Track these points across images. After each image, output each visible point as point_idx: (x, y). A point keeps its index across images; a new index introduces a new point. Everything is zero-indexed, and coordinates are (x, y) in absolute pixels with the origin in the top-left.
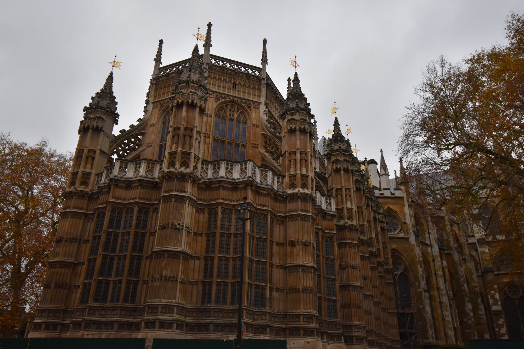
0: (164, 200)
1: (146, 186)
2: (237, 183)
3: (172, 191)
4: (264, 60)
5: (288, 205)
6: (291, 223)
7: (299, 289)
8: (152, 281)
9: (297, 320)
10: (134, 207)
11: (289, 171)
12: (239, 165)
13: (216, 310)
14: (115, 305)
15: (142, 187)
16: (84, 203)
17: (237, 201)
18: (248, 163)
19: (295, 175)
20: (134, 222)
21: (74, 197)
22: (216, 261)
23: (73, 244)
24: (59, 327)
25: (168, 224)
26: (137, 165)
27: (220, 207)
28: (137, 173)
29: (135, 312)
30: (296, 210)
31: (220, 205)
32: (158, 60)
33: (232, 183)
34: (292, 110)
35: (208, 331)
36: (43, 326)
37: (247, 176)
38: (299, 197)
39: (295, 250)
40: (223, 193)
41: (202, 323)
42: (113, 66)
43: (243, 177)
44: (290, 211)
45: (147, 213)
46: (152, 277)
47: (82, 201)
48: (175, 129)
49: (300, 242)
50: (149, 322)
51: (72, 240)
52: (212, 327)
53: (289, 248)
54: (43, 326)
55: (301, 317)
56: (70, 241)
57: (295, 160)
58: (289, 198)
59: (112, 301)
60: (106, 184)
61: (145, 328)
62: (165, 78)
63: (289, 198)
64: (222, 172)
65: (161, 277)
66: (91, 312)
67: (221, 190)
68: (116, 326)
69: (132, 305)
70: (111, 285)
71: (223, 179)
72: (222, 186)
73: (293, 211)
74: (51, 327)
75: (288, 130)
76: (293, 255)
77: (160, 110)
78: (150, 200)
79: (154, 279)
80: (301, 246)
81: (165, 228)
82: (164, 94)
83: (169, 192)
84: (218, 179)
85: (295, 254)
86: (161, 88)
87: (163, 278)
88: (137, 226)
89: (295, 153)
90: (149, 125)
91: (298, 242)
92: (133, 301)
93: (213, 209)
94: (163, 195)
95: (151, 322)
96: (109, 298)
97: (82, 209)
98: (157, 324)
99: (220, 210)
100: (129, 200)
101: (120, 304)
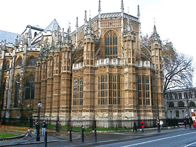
4: (138, 15)
20: (117, 80)
45: (119, 77)
88: (118, 81)
92: (120, 104)
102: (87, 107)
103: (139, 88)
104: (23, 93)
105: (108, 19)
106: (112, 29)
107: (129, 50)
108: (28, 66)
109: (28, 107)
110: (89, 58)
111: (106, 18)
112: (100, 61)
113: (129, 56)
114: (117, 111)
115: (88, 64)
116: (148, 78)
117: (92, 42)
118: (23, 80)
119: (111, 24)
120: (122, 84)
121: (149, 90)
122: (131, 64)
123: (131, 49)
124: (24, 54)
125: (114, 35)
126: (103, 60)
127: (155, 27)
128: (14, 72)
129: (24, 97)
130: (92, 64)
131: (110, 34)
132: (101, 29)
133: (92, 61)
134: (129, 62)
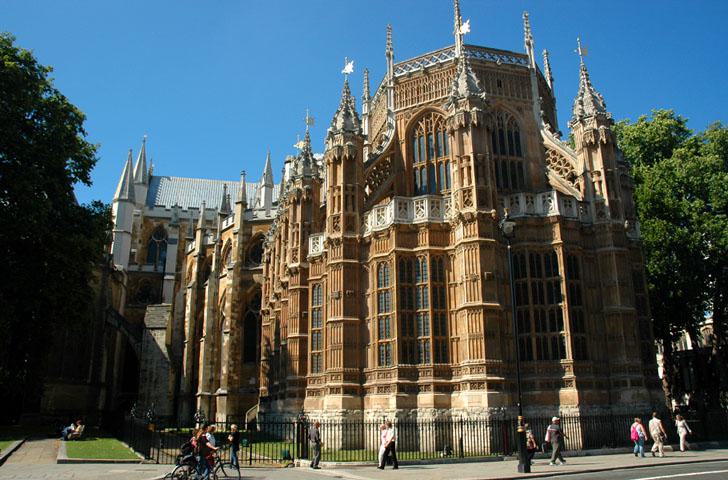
64: (523, 207)
102: (334, 375)
103: (520, 297)
104: (233, 345)
105: (416, 75)
106: (429, 106)
108: (247, 266)
109: (252, 386)
113: (466, 181)
114: (432, 387)
115: (336, 228)
118: (233, 306)
122: (473, 209)
123: (472, 159)
124: (235, 234)
125: (437, 125)
126: (383, 210)
128: (218, 286)
129: (239, 358)
134: (467, 203)
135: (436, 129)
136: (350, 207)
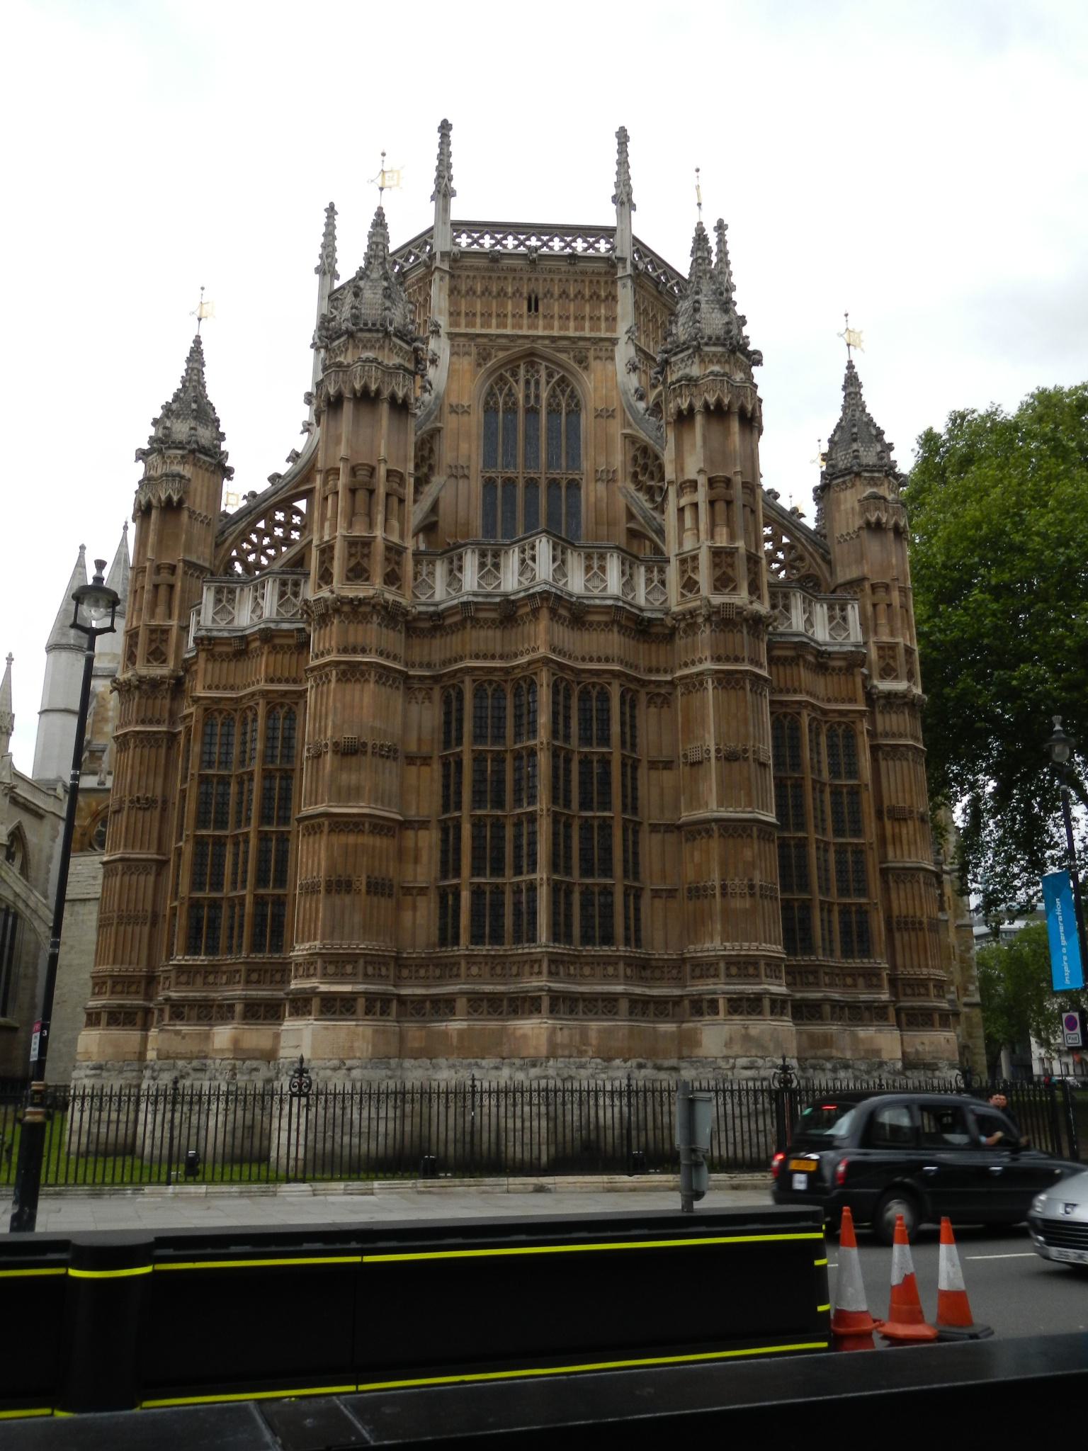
0: (719, 681)
1: (627, 627)
2: (830, 653)
3: (737, 660)
5: (879, 718)
6: (891, 763)
7: (921, 923)
8: (724, 895)
9: (922, 991)
10: (609, 684)
11: (876, 633)
12: (825, 606)
13: (827, 970)
14: (606, 950)
15: (623, 629)
16: (394, 639)
17: (829, 701)
18: (849, 607)
19: (893, 647)
20: (615, 728)
21: (375, 618)
22: (813, 850)
23: (388, 763)
24: (394, 1005)
25: (745, 751)
26: (589, 557)
27: (805, 713)
28: (528, 575)
29: (644, 968)
30: (901, 736)
31: (805, 707)
32: (443, 193)
33: (820, 654)
34: (872, 471)
35: (821, 1018)
36: (361, 1003)
37: (852, 639)
38: (906, 704)
39: (904, 831)
40: (805, 676)
41: (803, 1000)
42: (381, 189)
43: (840, 639)
44: (886, 735)
45: (633, 707)
46: (724, 887)
47: (391, 633)
48: (712, 482)
49: (915, 815)
50: (740, 999)
51: (388, 753)
52: (827, 1008)
53: (888, 824)
54: (361, 1003)
55: (931, 985)
56: (382, 756)
57: (889, 605)
58: (882, 702)
59: (587, 939)
60: (498, 600)
61: (730, 1013)
62: (483, 263)
63: (882, 702)
65: (752, 887)
66: (553, 968)
67: (802, 669)
68: (624, 1005)
69: (640, 953)
70: (576, 898)
71: (805, 640)
72: (803, 657)
73: (894, 736)
74: (378, 1005)
75: (868, 524)
76: (901, 841)
77: (479, 365)
78: (637, 668)
79: (730, 890)
80: (917, 823)
81: (737, 759)
82: (487, 316)
83: (728, 659)
84: (796, 639)
85: (905, 842)
86: (471, 291)
87: (757, 889)
89: (887, 587)
90: (446, 409)
91: (911, 812)
92: (638, 943)
93: (785, 715)
94: (708, 665)
95: (748, 999)
96: (576, 931)
97: (395, 658)
98: (766, 1003)
99: (805, 721)
100: (583, 659)
101: (622, 950)
106: (539, 345)
107: (721, 488)
110: (371, 526)
111: (494, 258)
112: (471, 562)
116: (850, 735)
117: (400, 394)
119: (533, 304)
120: (653, 765)
121: (858, 832)
125: (553, 395)
126: (496, 555)
127: (852, 383)
130: (392, 578)
131: (527, 382)
132: (452, 336)
133: (394, 551)
135: (549, 405)
136: (395, 523)
